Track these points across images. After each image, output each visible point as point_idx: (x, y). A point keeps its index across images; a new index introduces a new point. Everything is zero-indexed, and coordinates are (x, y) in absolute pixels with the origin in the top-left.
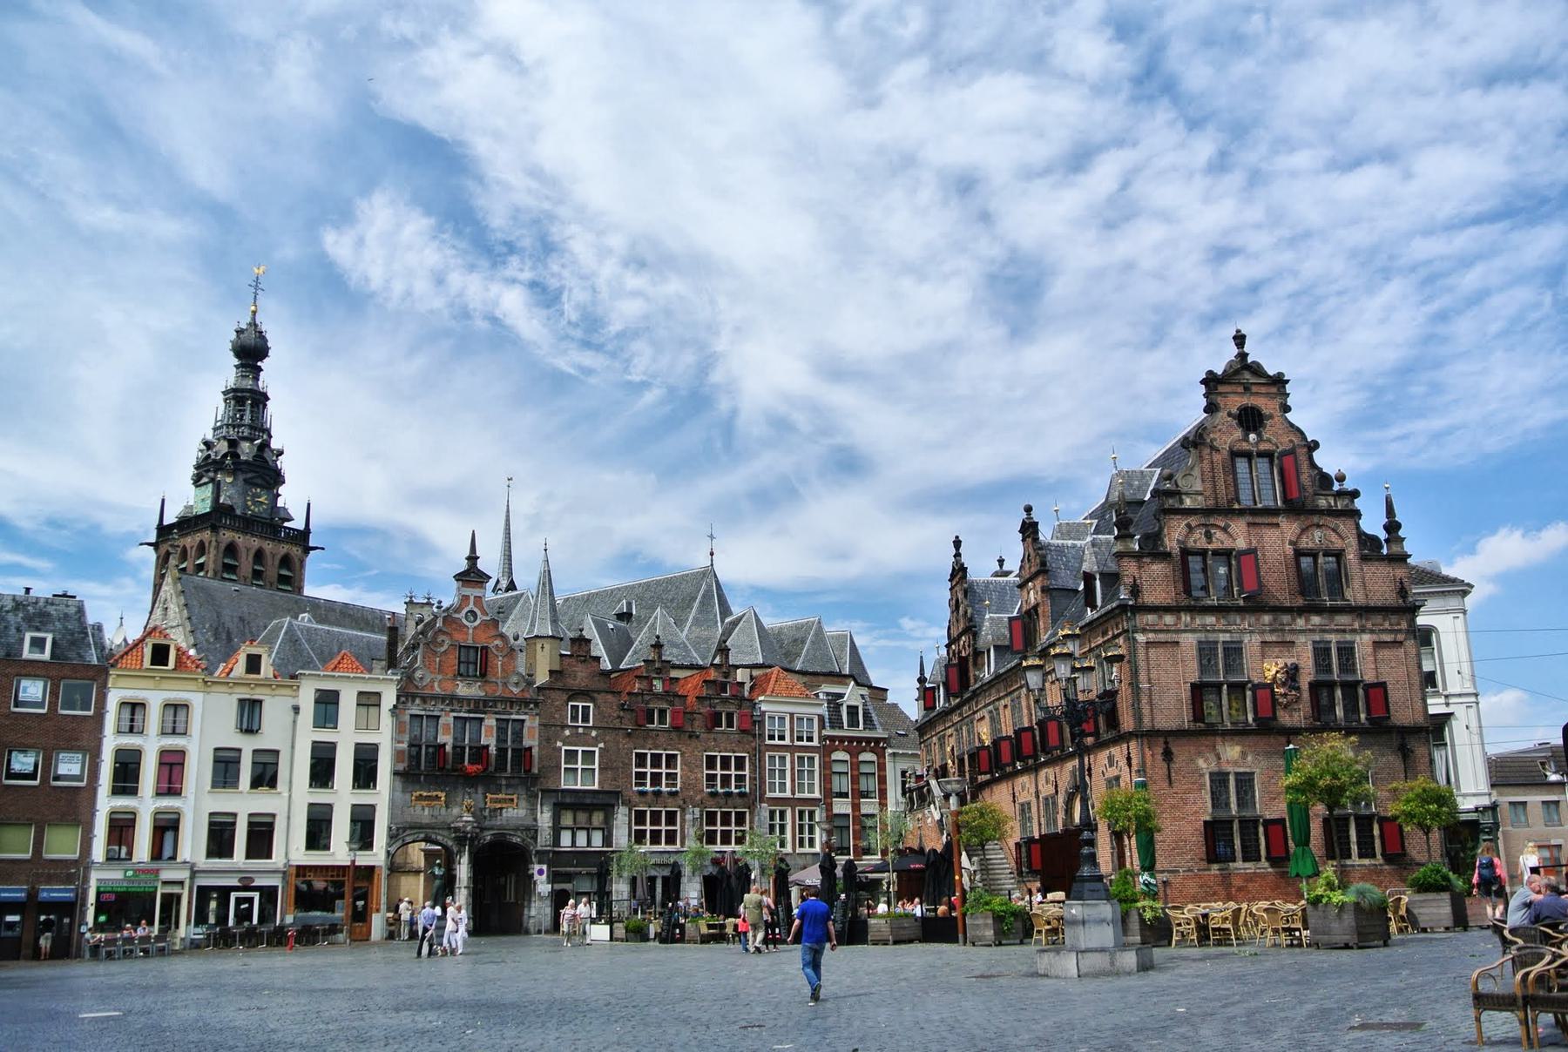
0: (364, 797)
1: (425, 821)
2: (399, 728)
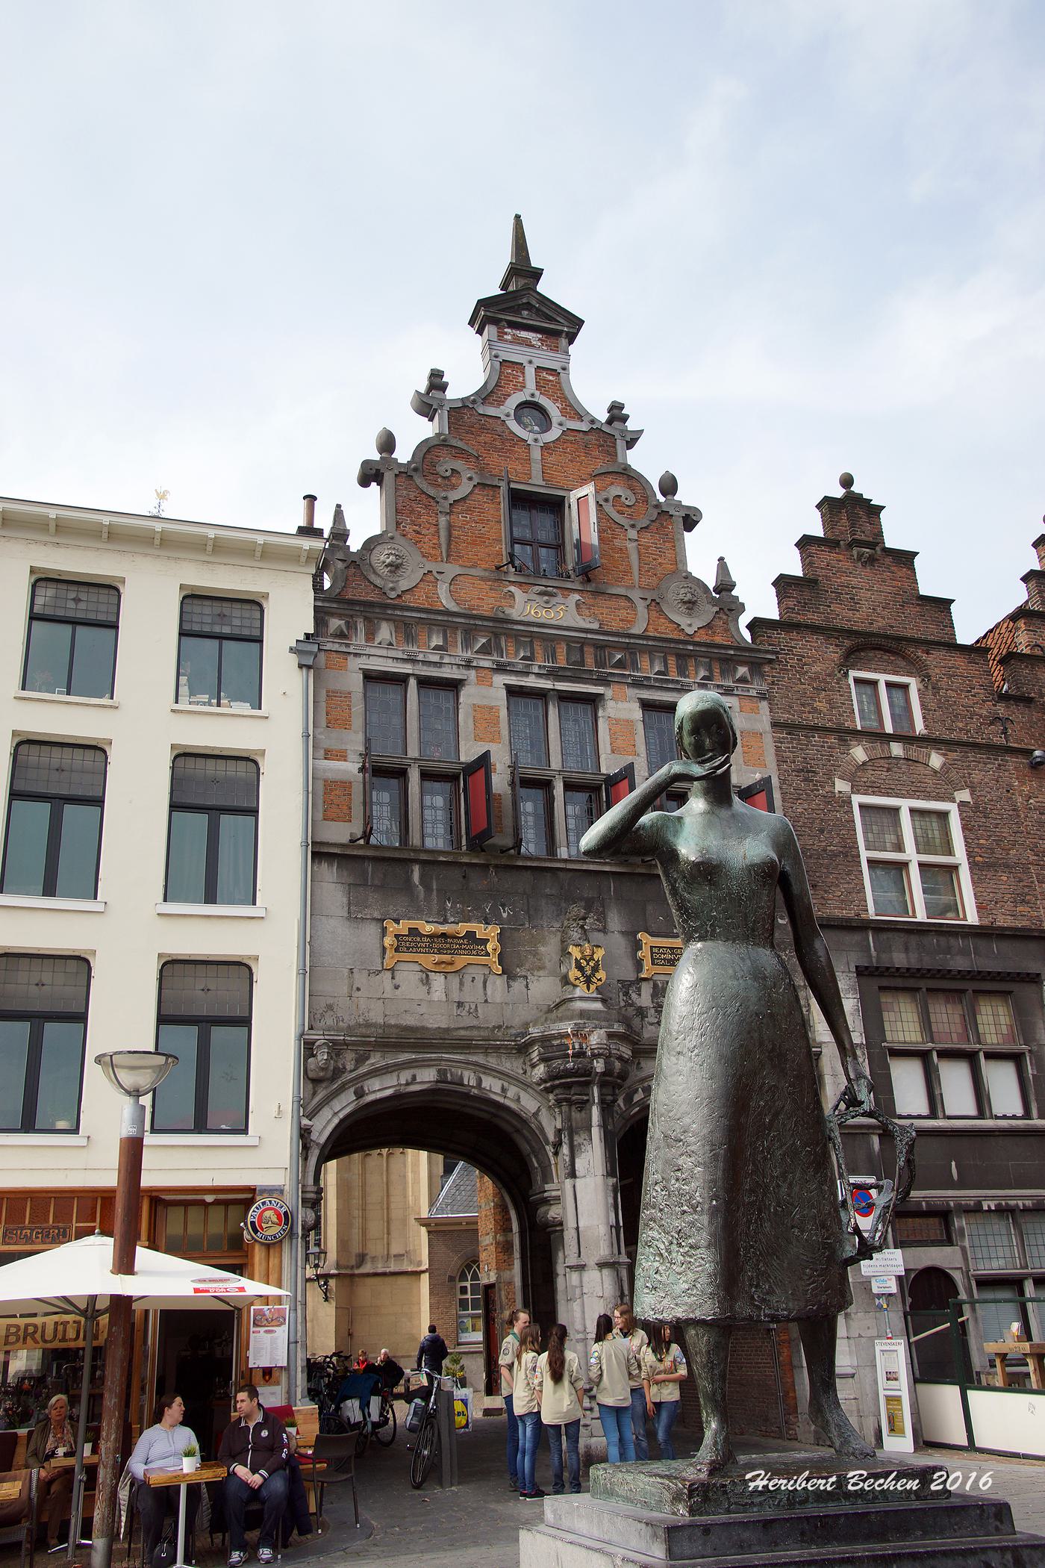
0: (207, 934)
1: (436, 1019)
2: (326, 711)
